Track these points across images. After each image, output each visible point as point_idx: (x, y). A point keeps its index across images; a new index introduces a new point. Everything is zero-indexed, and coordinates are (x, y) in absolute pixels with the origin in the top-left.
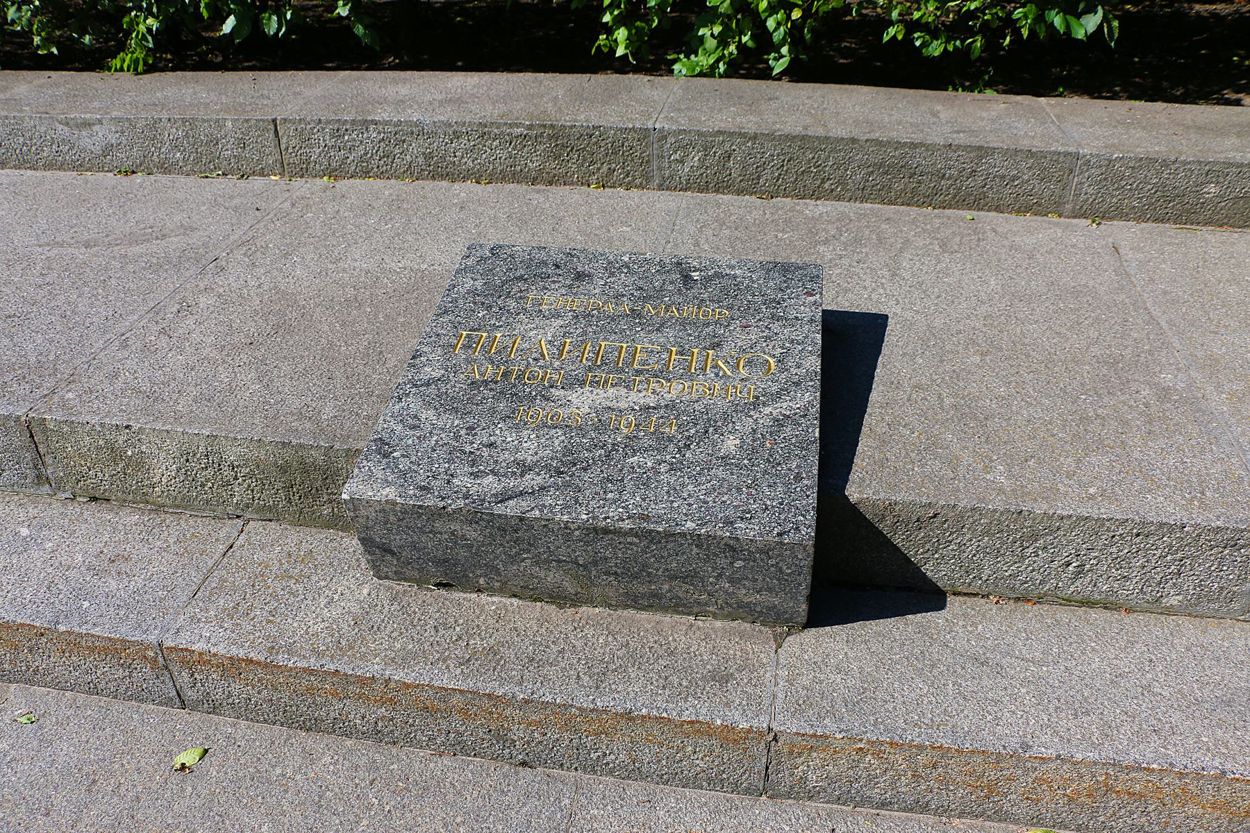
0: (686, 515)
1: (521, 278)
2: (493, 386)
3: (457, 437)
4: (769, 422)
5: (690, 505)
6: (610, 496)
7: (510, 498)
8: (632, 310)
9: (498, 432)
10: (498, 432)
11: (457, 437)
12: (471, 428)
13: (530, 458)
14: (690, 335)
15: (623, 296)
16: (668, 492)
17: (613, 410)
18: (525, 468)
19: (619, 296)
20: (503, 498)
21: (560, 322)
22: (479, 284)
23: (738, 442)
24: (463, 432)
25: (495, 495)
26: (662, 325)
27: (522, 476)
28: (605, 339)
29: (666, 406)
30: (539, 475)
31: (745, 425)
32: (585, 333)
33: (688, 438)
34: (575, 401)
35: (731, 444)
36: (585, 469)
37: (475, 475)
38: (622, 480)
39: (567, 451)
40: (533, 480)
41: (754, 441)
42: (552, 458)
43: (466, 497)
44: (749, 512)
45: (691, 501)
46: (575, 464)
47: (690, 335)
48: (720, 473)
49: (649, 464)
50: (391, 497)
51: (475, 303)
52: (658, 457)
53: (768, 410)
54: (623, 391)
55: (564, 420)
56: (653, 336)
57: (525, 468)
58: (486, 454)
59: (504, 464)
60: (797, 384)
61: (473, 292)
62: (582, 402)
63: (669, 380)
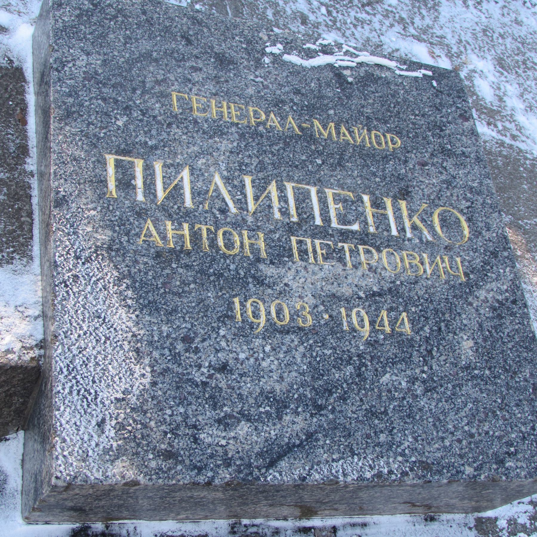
0: (461, 456)
1: (147, 56)
2: (185, 260)
3: (176, 357)
4: (485, 311)
5: (459, 441)
6: (382, 438)
7: (280, 457)
8: (300, 127)
9: (223, 344)
10: (223, 344)
11: (176, 357)
12: (187, 340)
13: (278, 387)
14: (374, 174)
15: (282, 102)
16: (434, 425)
17: (339, 299)
18: (281, 406)
19: (278, 103)
20: (273, 455)
21: (225, 145)
22: (96, 61)
23: (471, 343)
24: (180, 347)
25: (260, 455)
26: (341, 158)
27: (280, 418)
28: (290, 179)
29: (390, 290)
30: (298, 414)
31: (468, 318)
32: (262, 166)
33: (427, 339)
34: (294, 285)
35: (467, 346)
36: (343, 399)
37: (224, 423)
38: (385, 413)
39: (316, 372)
40: (295, 424)
41: (485, 340)
42: (302, 385)
43: (228, 463)
44: (512, 445)
45: (459, 434)
46: (331, 393)
47: (374, 174)
48: (468, 388)
49: (404, 384)
50: (131, 474)
51: (104, 100)
52: (408, 372)
53: (482, 294)
54: (339, 268)
55: (292, 319)
56: (339, 174)
57: (281, 406)
58: (223, 385)
59: (251, 401)
60: (495, 254)
61: (90, 76)
62: (303, 285)
63: (379, 251)
